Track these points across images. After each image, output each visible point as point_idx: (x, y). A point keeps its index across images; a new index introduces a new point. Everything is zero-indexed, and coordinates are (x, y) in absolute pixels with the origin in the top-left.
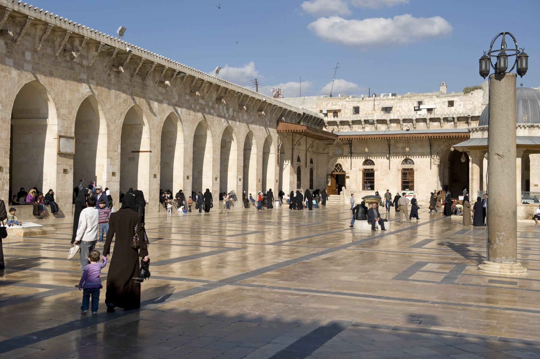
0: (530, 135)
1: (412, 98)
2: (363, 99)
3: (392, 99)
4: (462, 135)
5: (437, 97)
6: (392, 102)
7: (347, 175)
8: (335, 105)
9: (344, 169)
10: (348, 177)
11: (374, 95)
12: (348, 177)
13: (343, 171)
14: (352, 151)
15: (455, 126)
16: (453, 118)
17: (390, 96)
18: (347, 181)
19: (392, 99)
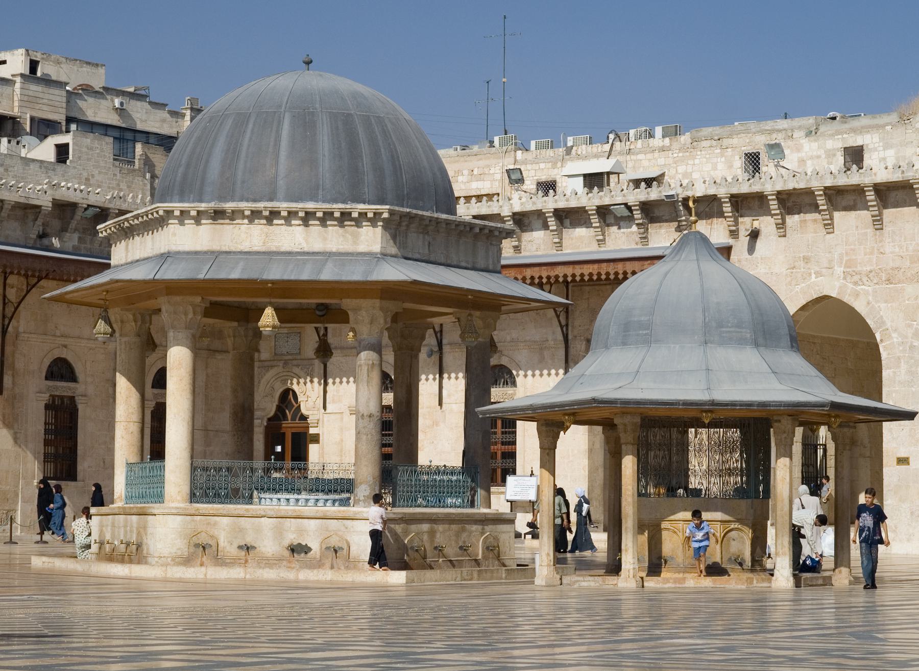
0: (216, 247)
1: (725, 142)
2: (569, 151)
3: (663, 149)
4: (586, 272)
5: (809, 134)
6: (661, 161)
7: (312, 431)
8: (481, 177)
9: (304, 411)
10: (316, 439)
11: (612, 136)
12: (316, 439)
13: (304, 418)
14: (331, 340)
15: (645, 238)
16: (628, 207)
17: (658, 140)
18: (313, 449)
19: (663, 149)
